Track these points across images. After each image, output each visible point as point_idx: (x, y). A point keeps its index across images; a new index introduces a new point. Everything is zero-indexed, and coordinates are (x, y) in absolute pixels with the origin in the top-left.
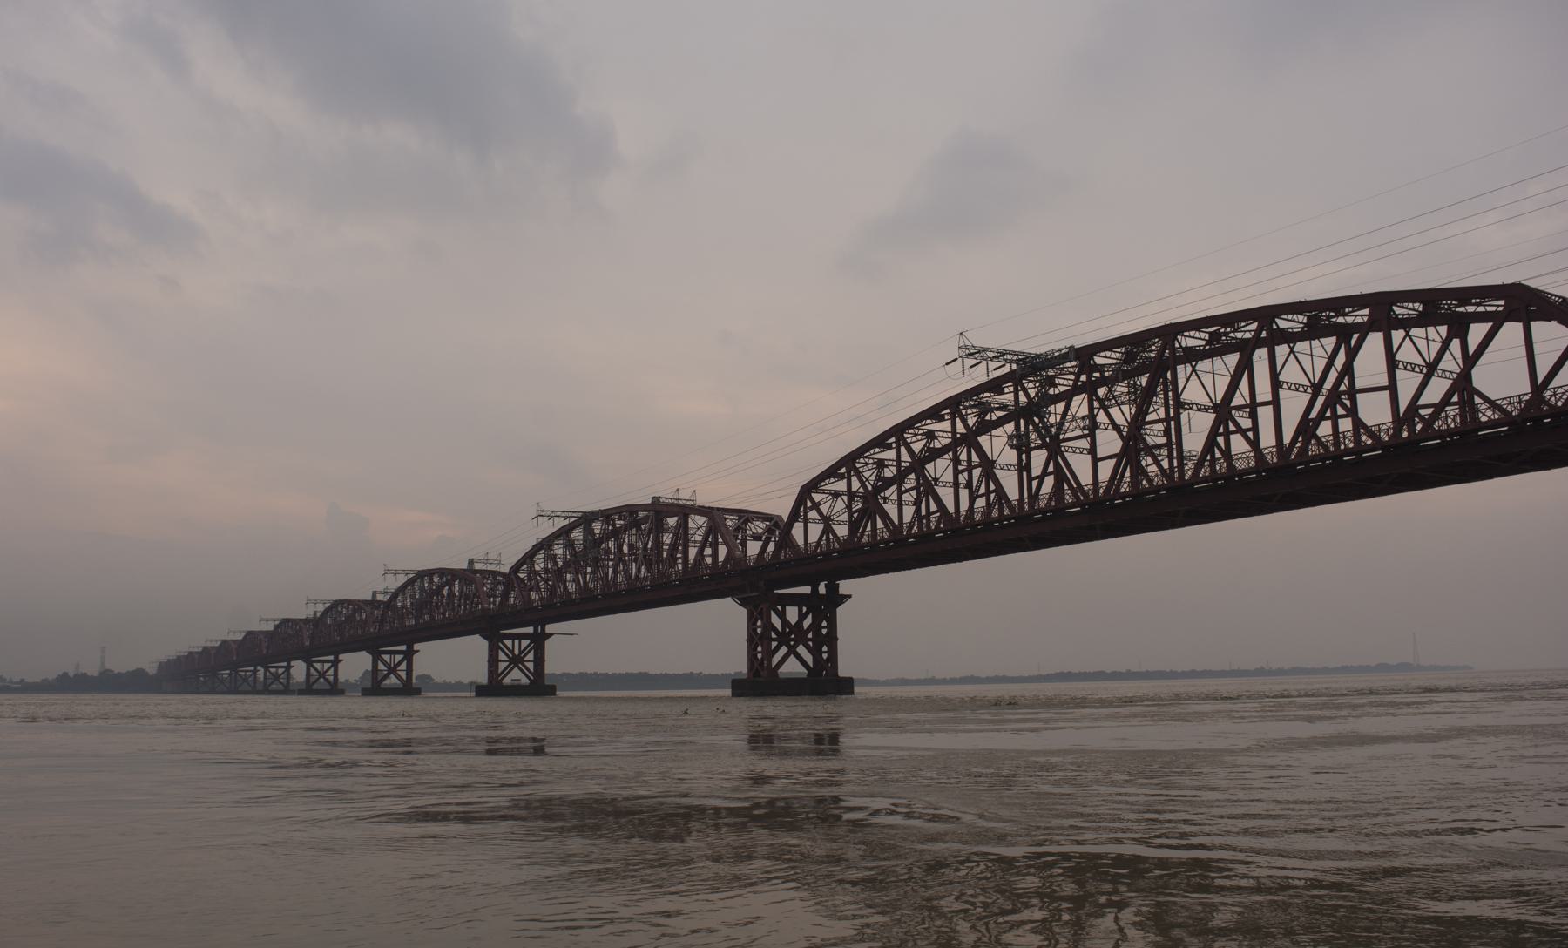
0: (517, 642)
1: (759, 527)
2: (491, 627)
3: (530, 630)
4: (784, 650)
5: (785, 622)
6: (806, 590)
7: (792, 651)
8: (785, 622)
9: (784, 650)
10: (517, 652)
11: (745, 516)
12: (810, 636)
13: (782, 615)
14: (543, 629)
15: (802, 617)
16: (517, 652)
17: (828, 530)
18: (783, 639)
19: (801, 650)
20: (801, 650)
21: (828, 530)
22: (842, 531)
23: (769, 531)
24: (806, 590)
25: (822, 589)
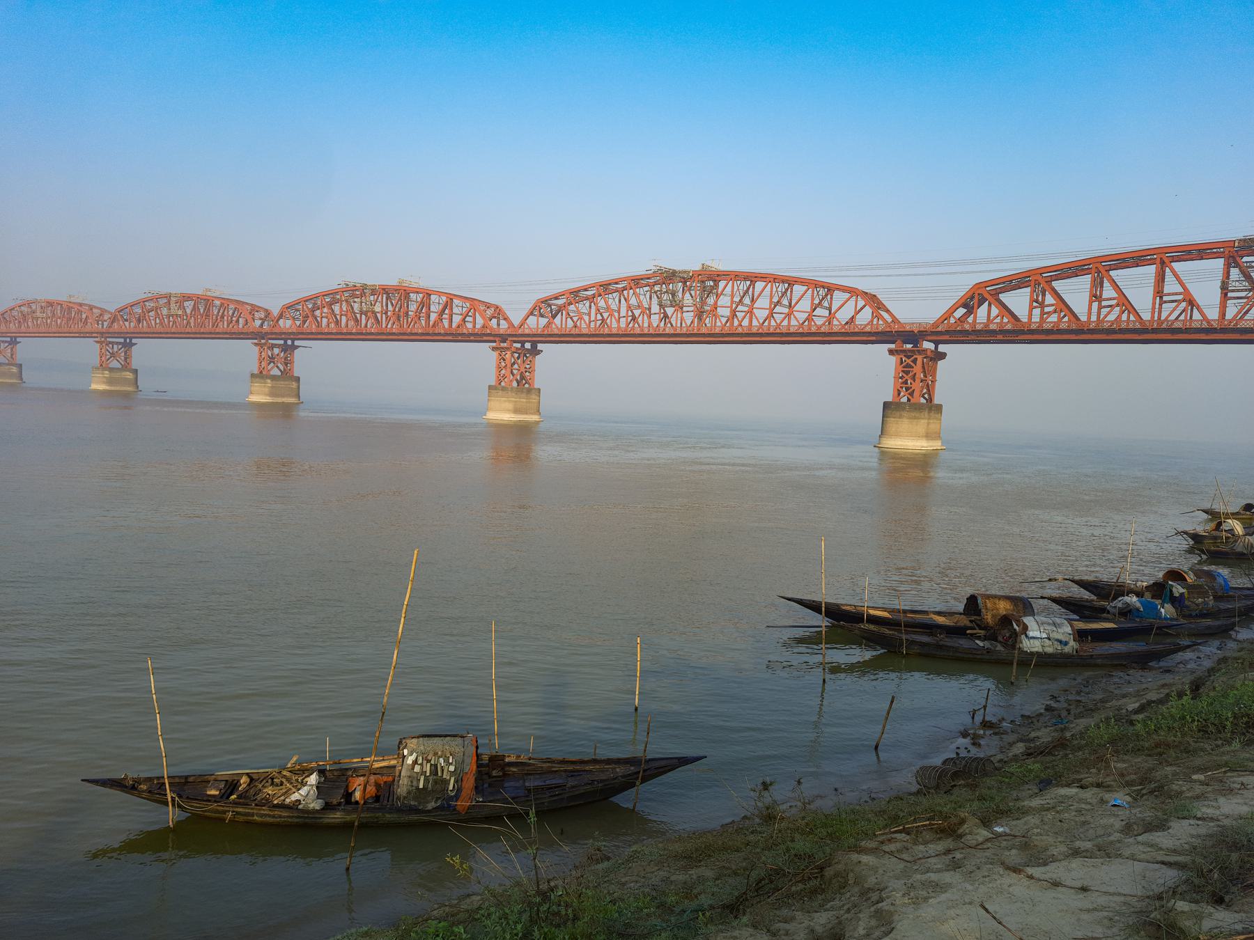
1: (106, 317)
12: (123, 354)
25: (128, 340)
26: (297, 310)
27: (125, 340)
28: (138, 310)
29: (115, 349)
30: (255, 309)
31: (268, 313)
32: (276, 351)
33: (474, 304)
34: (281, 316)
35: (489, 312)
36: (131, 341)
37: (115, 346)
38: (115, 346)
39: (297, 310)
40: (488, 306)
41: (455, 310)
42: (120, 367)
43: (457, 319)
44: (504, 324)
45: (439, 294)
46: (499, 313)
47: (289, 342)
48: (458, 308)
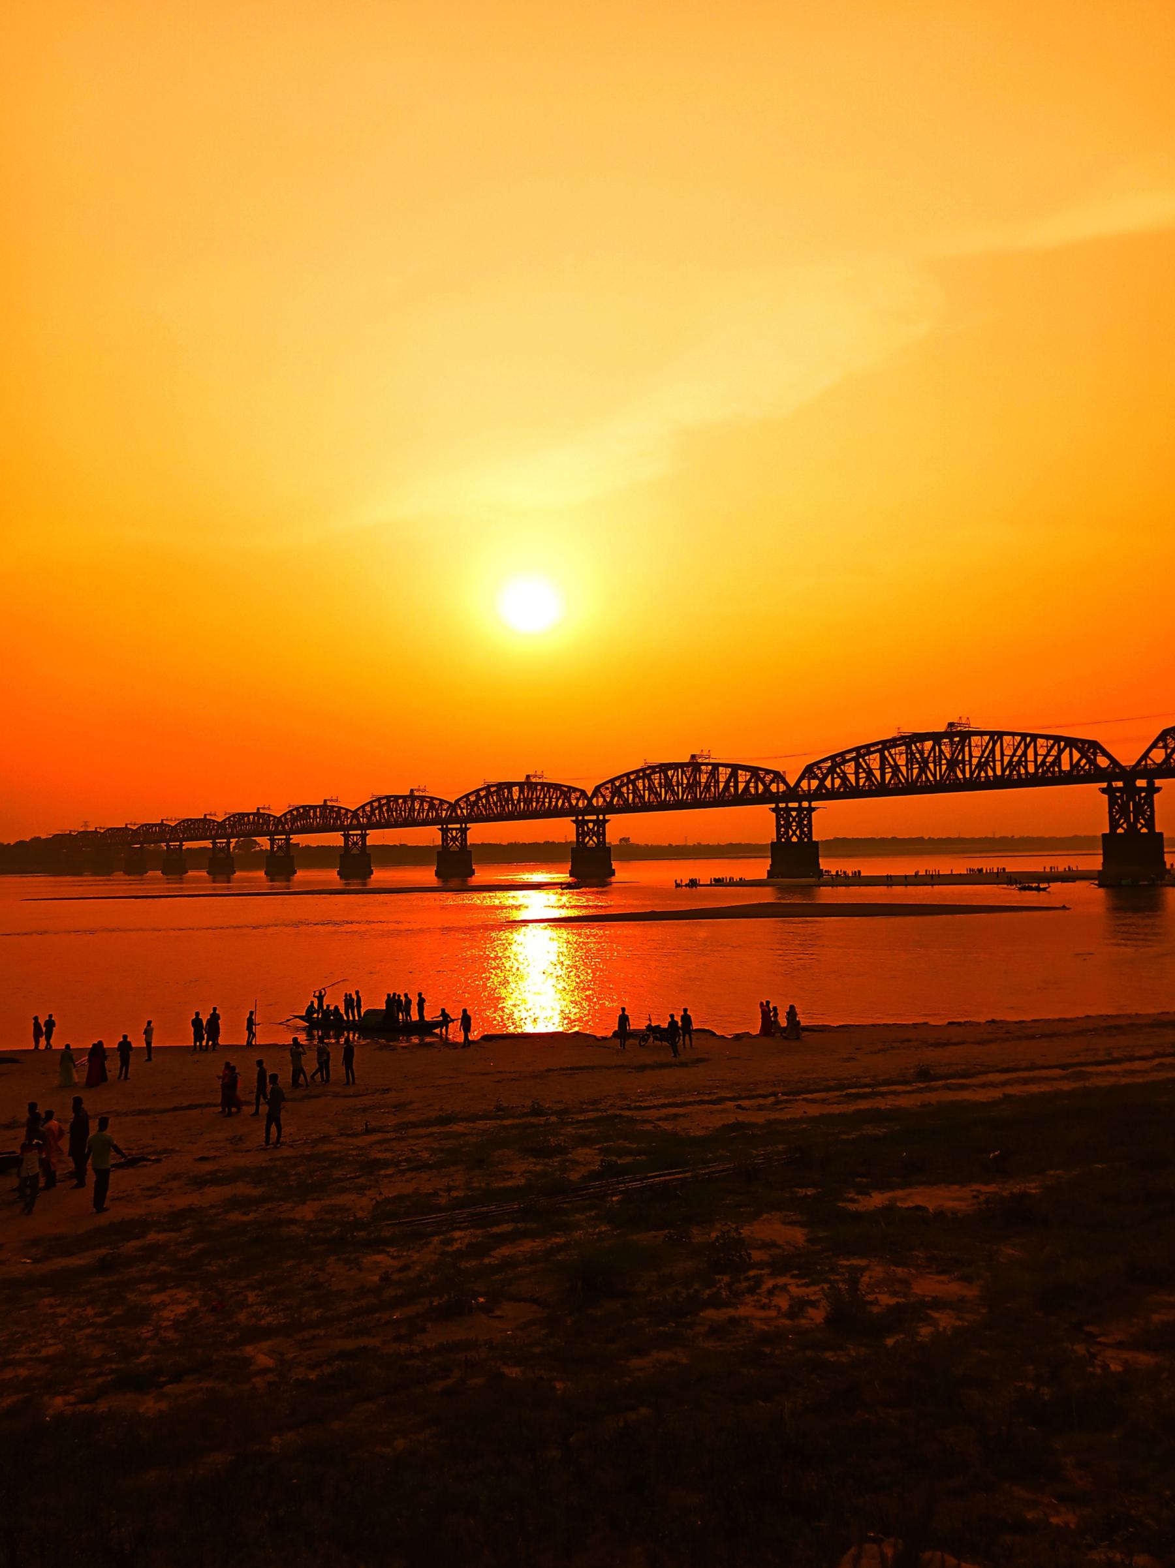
0: (355, 837)
1: (446, 806)
2: (345, 829)
3: (359, 832)
4: (452, 843)
5: (452, 836)
6: (458, 826)
7: (454, 843)
8: (452, 836)
9: (452, 843)
10: (355, 840)
11: (442, 802)
13: (451, 834)
14: (365, 832)
15: (457, 834)
16: (355, 840)
17: (462, 812)
18: (451, 840)
19: (457, 843)
20: (457, 843)
21: (462, 812)
22: (465, 811)
23: (448, 808)
24: (458, 826)
25: (464, 826)
26: (607, 788)
27: (461, 826)
28: (472, 798)
29: (454, 834)
30: (573, 789)
31: (583, 793)
32: (591, 825)
33: (754, 771)
34: (594, 794)
35: (768, 778)
36: (466, 826)
37: (454, 832)
38: (454, 832)
39: (607, 788)
40: (768, 772)
41: (740, 779)
42: (458, 849)
43: (741, 786)
44: (782, 787)
45: (726, 766)
46: (778, 777)
47: (601, 817)
48: (743, 776)
